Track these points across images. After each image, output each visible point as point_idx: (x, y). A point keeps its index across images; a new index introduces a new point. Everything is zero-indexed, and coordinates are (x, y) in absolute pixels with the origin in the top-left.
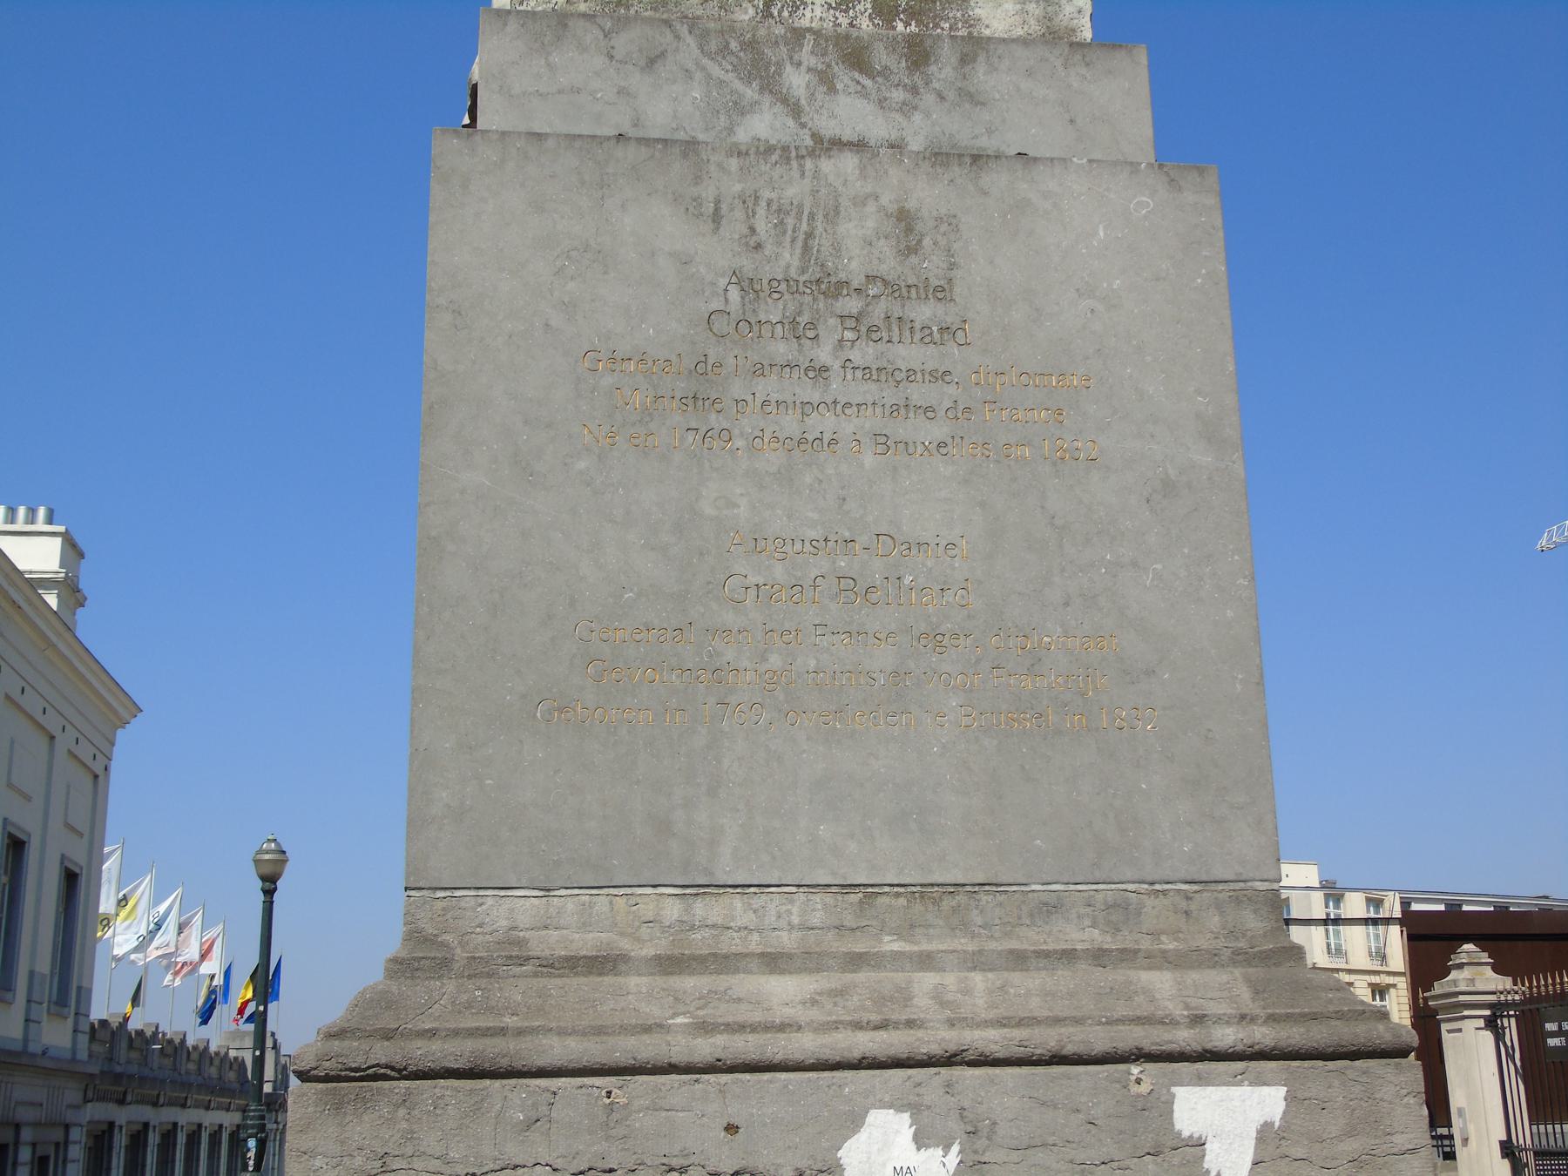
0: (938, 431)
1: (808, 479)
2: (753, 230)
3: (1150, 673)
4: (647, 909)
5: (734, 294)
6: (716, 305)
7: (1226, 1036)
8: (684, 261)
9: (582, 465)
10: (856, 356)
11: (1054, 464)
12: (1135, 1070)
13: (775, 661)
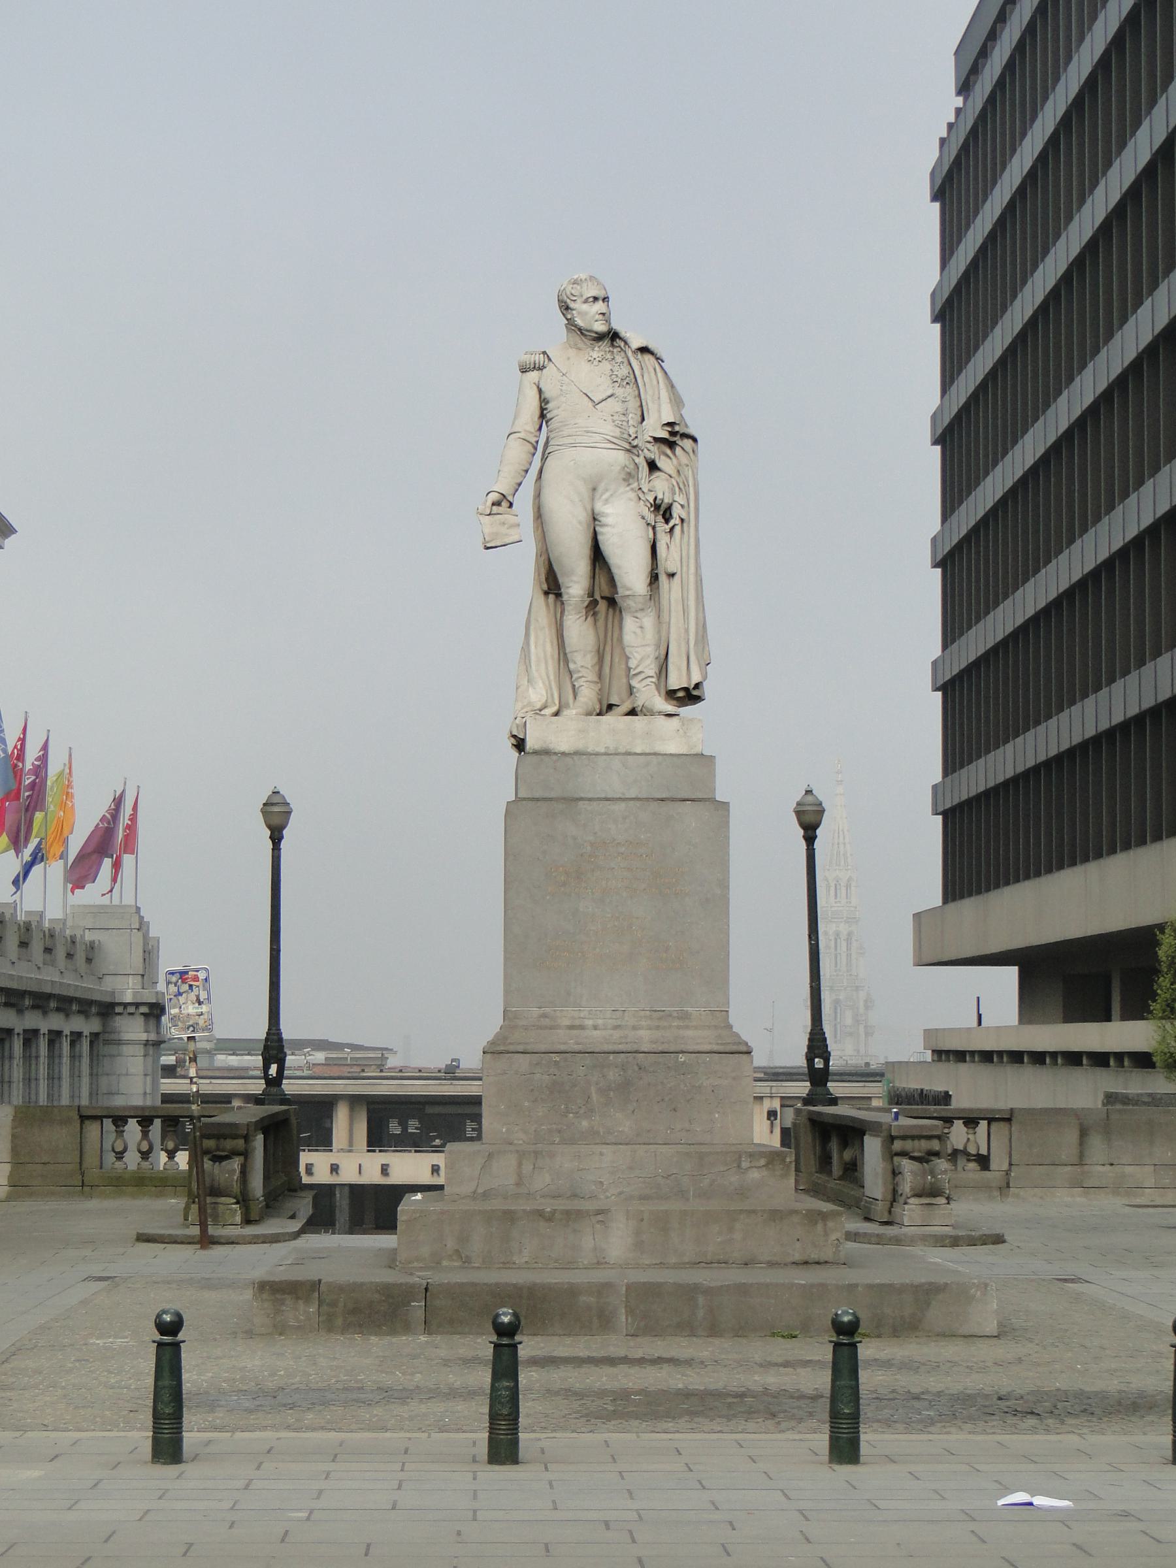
8: (575, 838)
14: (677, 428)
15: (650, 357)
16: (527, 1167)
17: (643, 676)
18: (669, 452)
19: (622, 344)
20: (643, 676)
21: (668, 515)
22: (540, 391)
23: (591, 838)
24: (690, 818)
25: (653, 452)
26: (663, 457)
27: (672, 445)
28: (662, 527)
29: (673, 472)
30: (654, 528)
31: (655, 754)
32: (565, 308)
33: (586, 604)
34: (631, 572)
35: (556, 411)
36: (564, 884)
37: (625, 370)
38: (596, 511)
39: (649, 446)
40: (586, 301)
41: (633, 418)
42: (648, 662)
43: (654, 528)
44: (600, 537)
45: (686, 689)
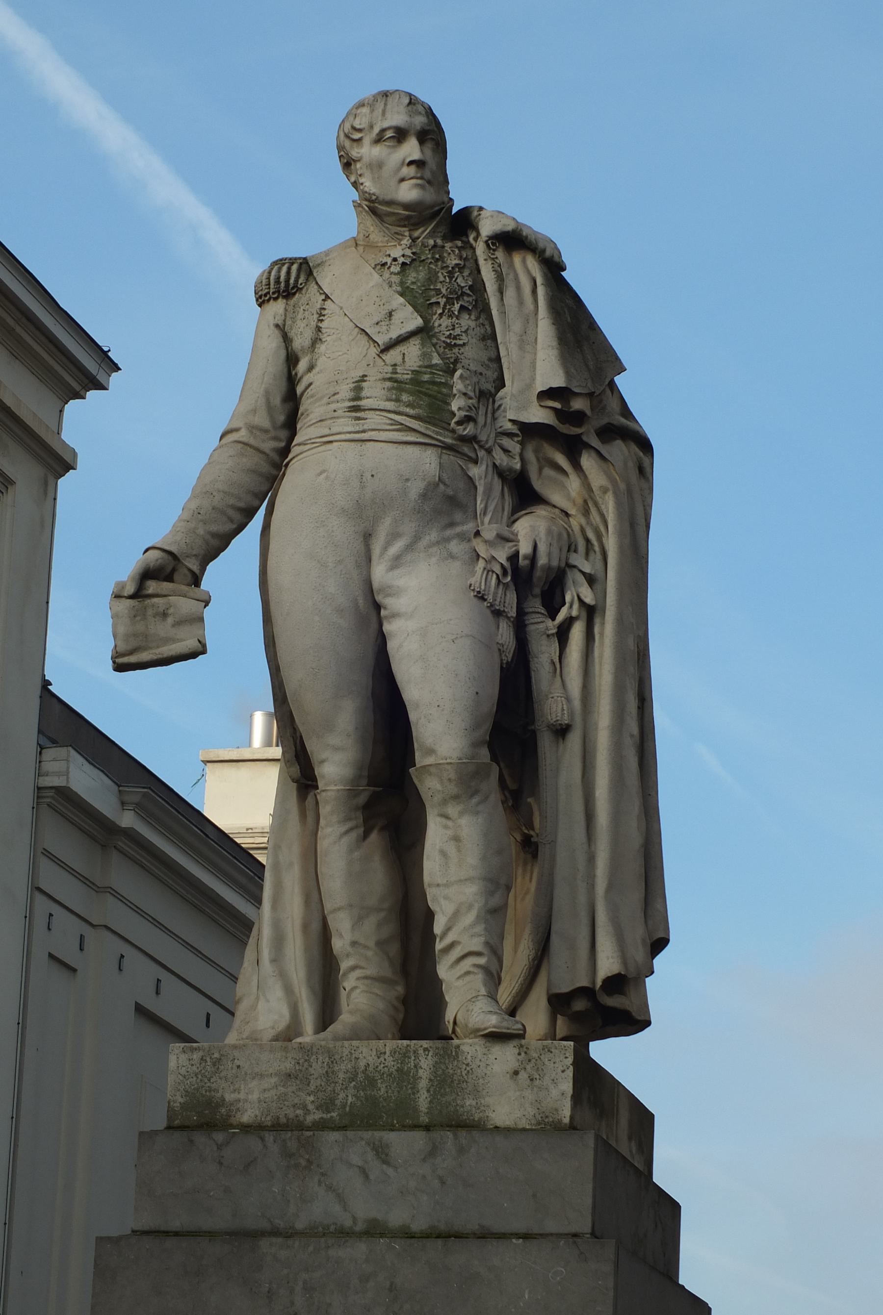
2: (292, 1303)
14: (578, 404)
17: (456, 953)
18: (561, 460)
20: (456, 953)
26: (548, 472)
27: (573, 448)
32: (348, 164)
33: (362, 799)
39: (507, 442)
40: (379, 139)
42: (469, 918)
44: (391, 646)
45: (586, 992)
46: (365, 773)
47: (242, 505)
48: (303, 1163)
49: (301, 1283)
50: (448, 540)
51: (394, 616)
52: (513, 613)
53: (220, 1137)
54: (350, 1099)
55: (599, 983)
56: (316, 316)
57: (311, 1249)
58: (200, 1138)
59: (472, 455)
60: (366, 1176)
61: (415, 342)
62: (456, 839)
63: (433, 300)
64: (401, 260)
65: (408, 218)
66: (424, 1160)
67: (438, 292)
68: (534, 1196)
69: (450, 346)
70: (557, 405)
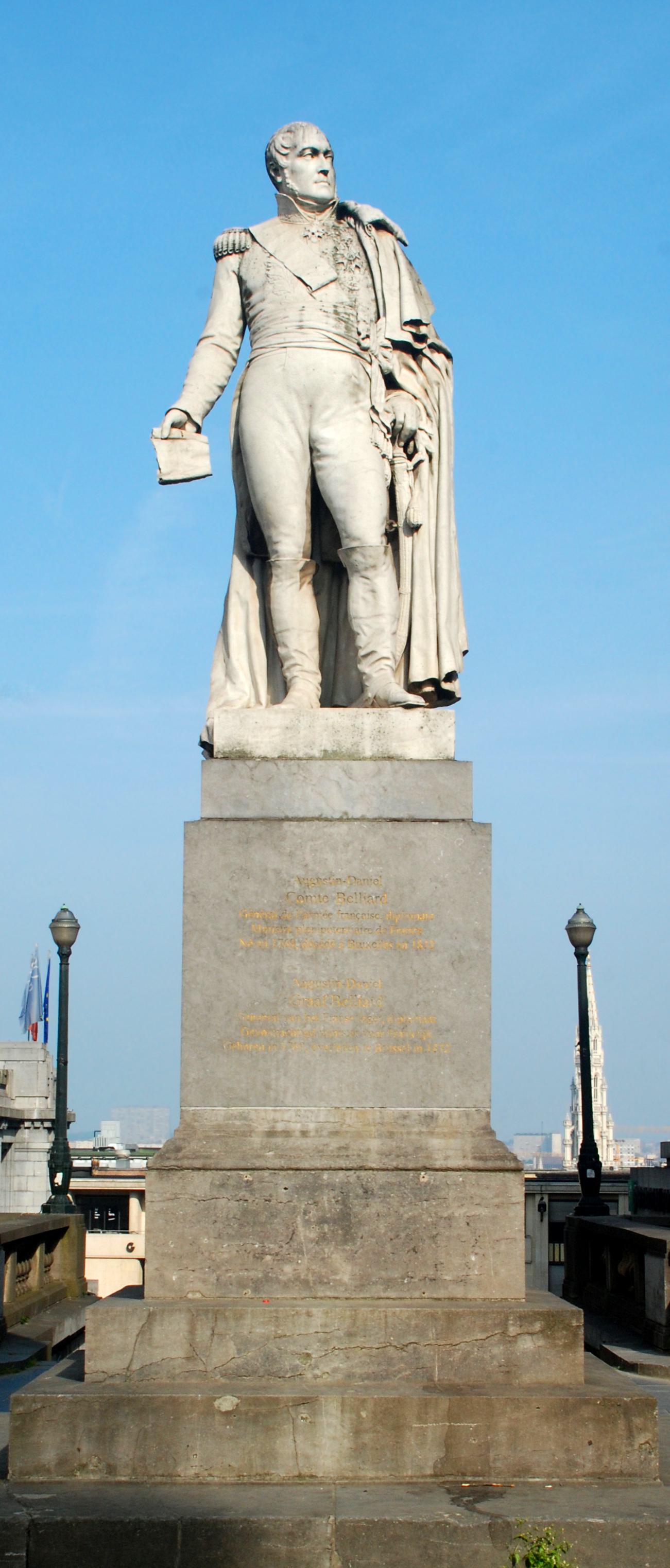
0: (372, 938)
1: (323, 958)
2: (304, 859)
3: (448, 1031)
4: (263, 1114)
5: (297, 885)
6: (290, 890)
7: (452, 1163)
8: (277, 872)
9: (240, 954)
10: (343, 909)
11: (417, 950)
12: (423, 1173)
13: (309, 1027)
14: (423, 330)
15: (389, 235)
16: (203, 1333)
19: (352, 221)
21: (410, 450)
22: (241, 281)
23: (301, 872)
24: (436, 844)
25: (395, 361)
26: (405, 372)
27: (416, 355)
28: (403, 464)
29: (419, 393)
30: (392, 464)
31: (390, 758)
34: (363, 522)
35: (265, 306)
36: (263, 936)
37: (355, 249)
38: (313, 437)
39: (387, 352)
41: (366, 311)
43: (392, 464)
44: (319, 474)
45: (434, 682)
46: (302, 550)
47: (220, 384)
48: (302, 778)
49: (309, 847)
50: (355, 411)
51: (324, 456)
52: (390, 457)
53: (251, 763)
54: (324, 742)
55: (443, 676)
56: (264, 267)
57: (314, 828)
58: (239, 764)
59: (369, 360)
60: (340, 786)
61: (332, 285)
62: (373, 591)
63: (340, 261)
64: (317, 234)
65: (317, 207)
66: (374, 777)
67: (343, 256)
68: (439, 798)
69: (351, 290)
70: (414, 330)
